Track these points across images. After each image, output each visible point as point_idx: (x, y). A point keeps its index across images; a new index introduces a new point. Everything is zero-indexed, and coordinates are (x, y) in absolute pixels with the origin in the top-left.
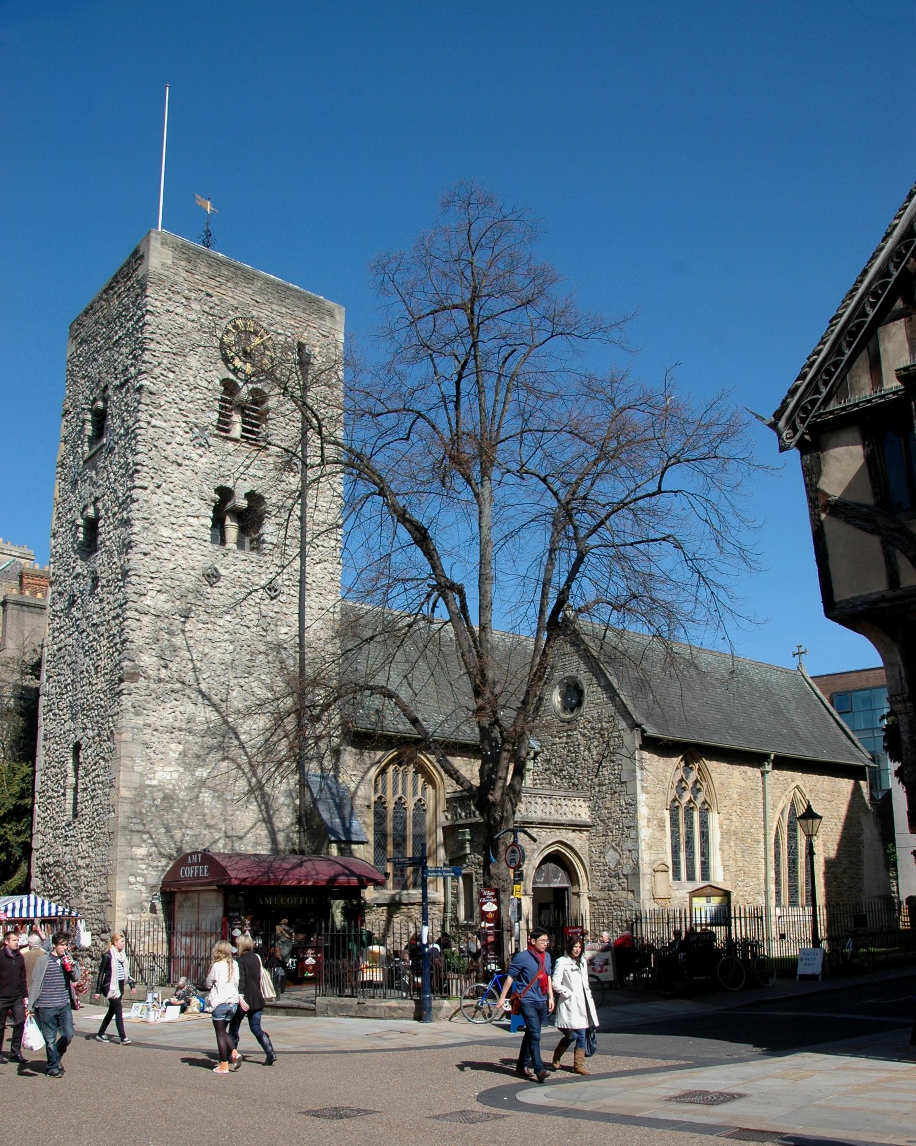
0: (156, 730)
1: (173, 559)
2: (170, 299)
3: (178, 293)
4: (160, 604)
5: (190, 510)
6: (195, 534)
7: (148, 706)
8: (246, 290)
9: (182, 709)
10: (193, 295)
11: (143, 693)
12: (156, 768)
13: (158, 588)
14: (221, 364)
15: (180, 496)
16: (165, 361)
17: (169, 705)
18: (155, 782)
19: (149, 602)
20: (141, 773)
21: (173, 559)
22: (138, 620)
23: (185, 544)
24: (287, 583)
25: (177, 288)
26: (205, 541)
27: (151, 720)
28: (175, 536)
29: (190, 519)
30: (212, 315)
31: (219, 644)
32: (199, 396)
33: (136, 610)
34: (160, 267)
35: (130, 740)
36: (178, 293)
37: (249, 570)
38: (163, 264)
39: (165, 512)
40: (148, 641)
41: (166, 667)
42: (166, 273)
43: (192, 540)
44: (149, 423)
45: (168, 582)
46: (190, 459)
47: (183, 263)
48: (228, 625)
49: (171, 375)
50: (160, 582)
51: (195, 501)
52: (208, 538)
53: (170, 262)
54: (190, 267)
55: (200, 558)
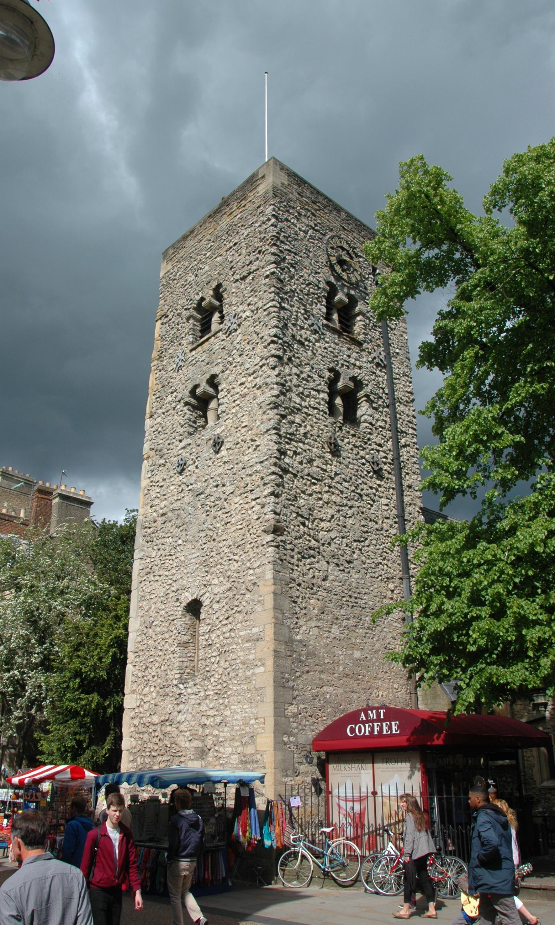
0: (299, 585)
1: (303, 424)
2: (288, 211)
3: (294, 208)
4: (296, 464)
5: (311, 385)
6: (317, 406)
7: (293, 561)
8: (337, 218)
9: (317, 565)
10: (303, 212)
11: (288, 547)
12: (301, 622)
13: (294, 449)
14: (326, 270)
15: (305, 370)
16: (287, 257)
17: (308, 561)
18: (299, 637)
19: (287, 460)
20: (289, 627)
21: (303, 424)
22: (281, 477)
23: (311, 413)
24: (384, 460)
25: (292, 204)
26: (326, 413)
27: (295, 575)
28: (304, 404)
29: (313, 393)
30: (316, 231)
31: (341, 508)
32: (311, 290)
33: (280, 467)
34: (280, 185)
35: (280, 592)
36: (294, 208)
37: (358, 444)
38: (283, 184)
39: (295, 381)
40: (289, 497)
41: (304, 524)
42: (285, 190)
43: (316, 411)
44: (280, 303)
45: (301, 445)
46: (309, 341)
47: (295, 187)
48: (345, 491)
49: (293, 270)
50: (295, 444)
51: (315, 377)
52: (327, 410)
53: (286, 183)
54: (300, 190)
55: (323, 427)
